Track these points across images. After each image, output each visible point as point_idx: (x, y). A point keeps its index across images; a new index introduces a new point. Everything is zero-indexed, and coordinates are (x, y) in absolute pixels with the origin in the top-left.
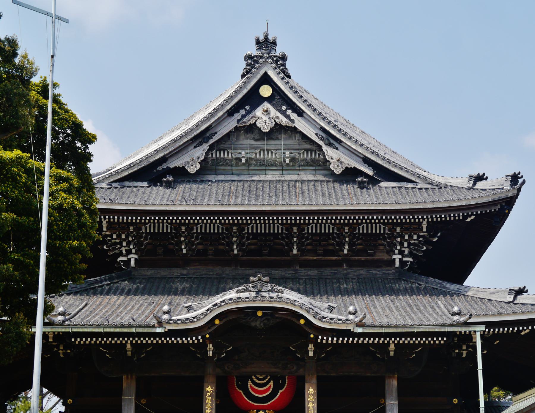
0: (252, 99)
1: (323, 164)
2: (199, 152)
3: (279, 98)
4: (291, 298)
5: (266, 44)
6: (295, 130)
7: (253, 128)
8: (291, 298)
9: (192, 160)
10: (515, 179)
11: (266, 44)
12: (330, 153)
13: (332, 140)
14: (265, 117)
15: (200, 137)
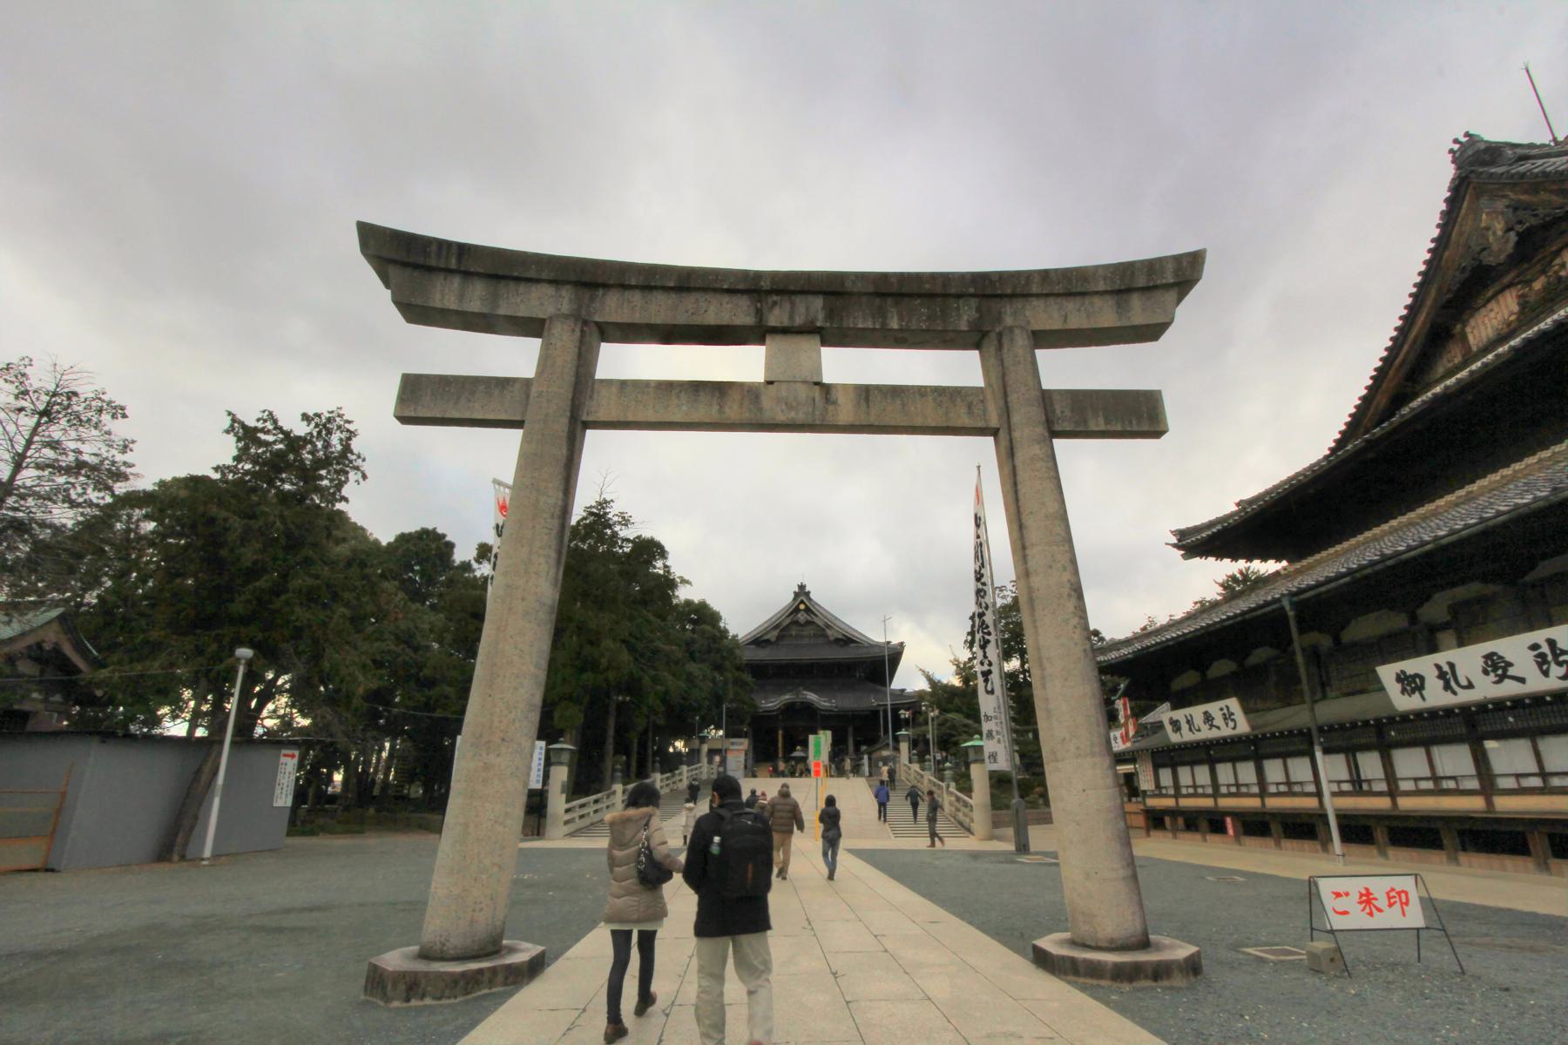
0: (797, 610)
1: (826, 636)
2: (776, 633)
3: (808, 610)
4: (812, 697)
5: (802, 587)
6: (813, 623)
7: (796, 623)
8: (812, 697)
9: (773, 636)
10: (902, 645)
11: (802, 587)
12: (829, 632)
13: (828, 626)
14: (802, 617)
15: (776, 627)
